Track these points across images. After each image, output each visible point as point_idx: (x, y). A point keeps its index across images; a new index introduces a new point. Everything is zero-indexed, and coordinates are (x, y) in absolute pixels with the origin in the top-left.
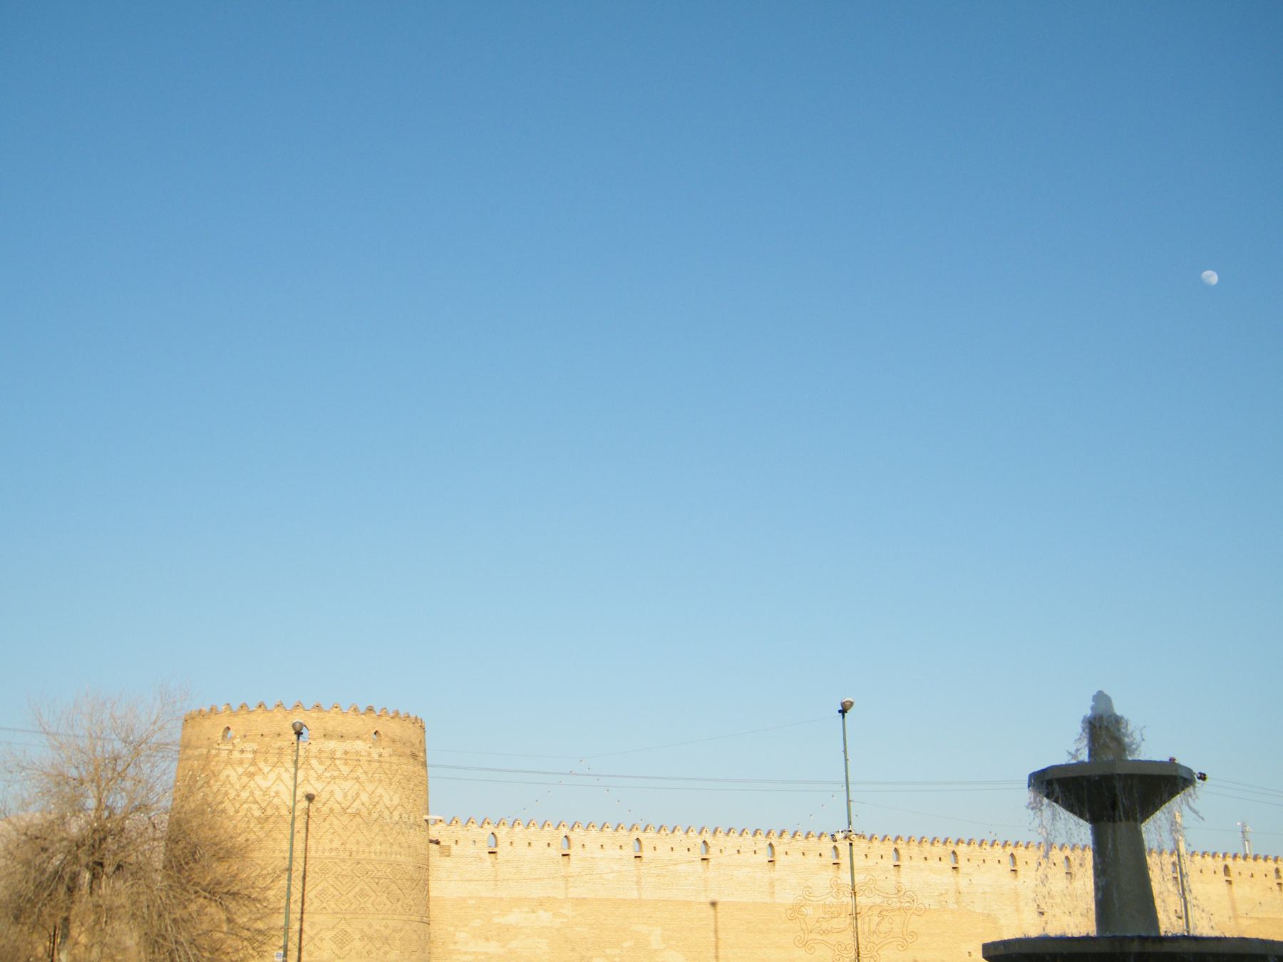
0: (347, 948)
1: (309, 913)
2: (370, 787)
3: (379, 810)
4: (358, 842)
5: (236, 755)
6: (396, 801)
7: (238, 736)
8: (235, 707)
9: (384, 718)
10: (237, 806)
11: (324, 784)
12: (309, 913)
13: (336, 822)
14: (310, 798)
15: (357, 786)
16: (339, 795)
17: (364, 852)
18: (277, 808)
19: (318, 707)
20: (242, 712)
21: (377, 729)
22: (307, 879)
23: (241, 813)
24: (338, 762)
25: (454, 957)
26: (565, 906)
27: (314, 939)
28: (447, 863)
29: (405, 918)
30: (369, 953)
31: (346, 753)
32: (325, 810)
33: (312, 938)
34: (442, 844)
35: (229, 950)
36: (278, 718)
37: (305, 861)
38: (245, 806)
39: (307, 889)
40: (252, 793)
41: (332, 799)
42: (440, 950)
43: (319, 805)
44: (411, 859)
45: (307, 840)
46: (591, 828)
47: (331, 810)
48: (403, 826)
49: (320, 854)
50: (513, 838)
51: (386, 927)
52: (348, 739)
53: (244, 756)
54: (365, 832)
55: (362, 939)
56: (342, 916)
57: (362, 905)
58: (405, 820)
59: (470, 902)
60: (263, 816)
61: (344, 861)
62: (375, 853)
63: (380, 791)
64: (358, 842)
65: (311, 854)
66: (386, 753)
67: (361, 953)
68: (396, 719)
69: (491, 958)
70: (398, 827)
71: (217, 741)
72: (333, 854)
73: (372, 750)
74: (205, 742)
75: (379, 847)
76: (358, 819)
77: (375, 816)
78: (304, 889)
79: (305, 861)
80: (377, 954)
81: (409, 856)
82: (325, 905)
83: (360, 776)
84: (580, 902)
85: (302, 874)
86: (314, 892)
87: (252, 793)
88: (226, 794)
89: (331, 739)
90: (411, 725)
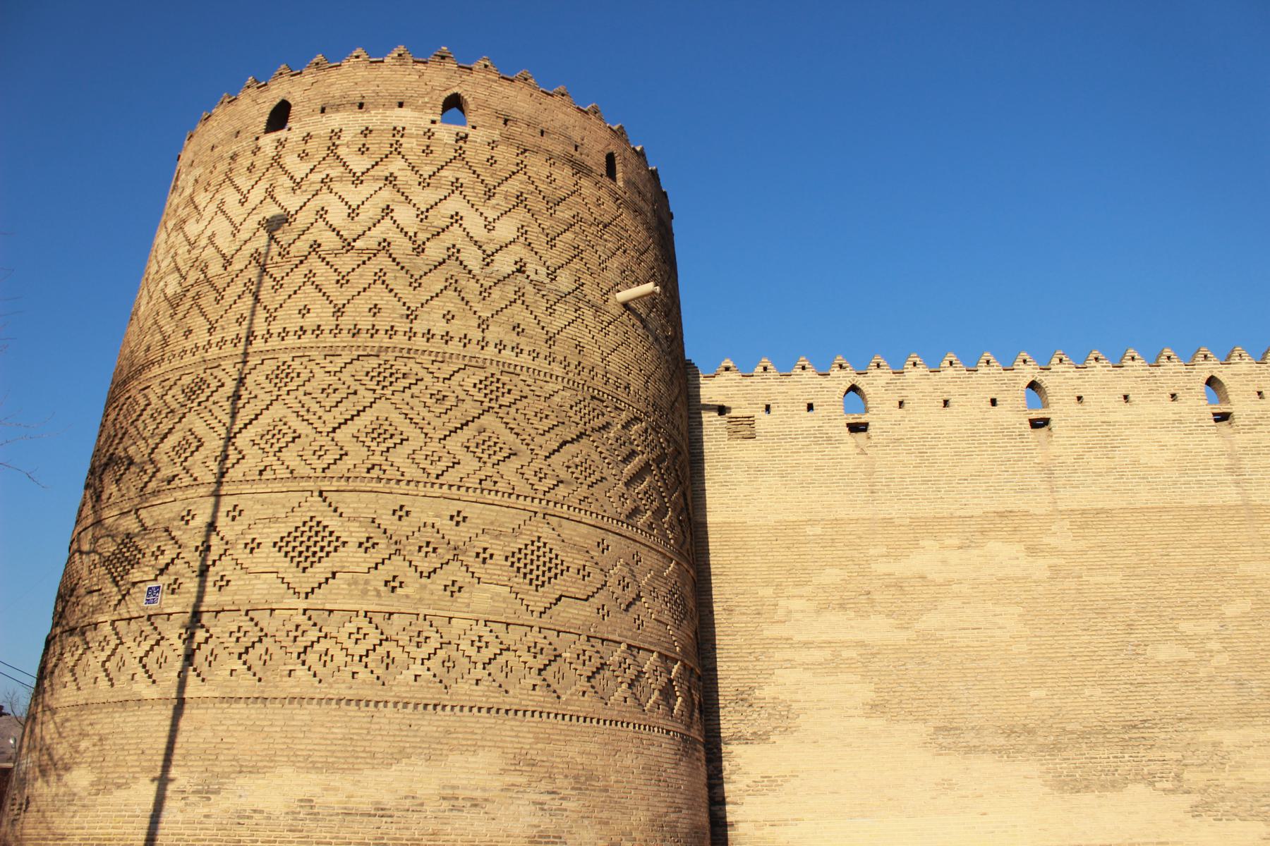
0: (320, 571)
2: (423, 198)
4: (375, 310)
6: (506, 229)
13: (320, 268)
16: (337, 215)
24: (342, 151)
25: (778, 656)
28: (746, 451)
30: (393, 584)
34: (733, 413)
42: (740, 641)
46: (1093, 363)
47: (315, 246)
50: (904, 393)
52: (376, 107)
55: (367, 545)
57: (377, 459)
59: (809, 530)
62: (429, 336)
67: (367, 582)
69: (874, 655)
76: (383, 260)
77: (435, 251)
84: (1087, 519)
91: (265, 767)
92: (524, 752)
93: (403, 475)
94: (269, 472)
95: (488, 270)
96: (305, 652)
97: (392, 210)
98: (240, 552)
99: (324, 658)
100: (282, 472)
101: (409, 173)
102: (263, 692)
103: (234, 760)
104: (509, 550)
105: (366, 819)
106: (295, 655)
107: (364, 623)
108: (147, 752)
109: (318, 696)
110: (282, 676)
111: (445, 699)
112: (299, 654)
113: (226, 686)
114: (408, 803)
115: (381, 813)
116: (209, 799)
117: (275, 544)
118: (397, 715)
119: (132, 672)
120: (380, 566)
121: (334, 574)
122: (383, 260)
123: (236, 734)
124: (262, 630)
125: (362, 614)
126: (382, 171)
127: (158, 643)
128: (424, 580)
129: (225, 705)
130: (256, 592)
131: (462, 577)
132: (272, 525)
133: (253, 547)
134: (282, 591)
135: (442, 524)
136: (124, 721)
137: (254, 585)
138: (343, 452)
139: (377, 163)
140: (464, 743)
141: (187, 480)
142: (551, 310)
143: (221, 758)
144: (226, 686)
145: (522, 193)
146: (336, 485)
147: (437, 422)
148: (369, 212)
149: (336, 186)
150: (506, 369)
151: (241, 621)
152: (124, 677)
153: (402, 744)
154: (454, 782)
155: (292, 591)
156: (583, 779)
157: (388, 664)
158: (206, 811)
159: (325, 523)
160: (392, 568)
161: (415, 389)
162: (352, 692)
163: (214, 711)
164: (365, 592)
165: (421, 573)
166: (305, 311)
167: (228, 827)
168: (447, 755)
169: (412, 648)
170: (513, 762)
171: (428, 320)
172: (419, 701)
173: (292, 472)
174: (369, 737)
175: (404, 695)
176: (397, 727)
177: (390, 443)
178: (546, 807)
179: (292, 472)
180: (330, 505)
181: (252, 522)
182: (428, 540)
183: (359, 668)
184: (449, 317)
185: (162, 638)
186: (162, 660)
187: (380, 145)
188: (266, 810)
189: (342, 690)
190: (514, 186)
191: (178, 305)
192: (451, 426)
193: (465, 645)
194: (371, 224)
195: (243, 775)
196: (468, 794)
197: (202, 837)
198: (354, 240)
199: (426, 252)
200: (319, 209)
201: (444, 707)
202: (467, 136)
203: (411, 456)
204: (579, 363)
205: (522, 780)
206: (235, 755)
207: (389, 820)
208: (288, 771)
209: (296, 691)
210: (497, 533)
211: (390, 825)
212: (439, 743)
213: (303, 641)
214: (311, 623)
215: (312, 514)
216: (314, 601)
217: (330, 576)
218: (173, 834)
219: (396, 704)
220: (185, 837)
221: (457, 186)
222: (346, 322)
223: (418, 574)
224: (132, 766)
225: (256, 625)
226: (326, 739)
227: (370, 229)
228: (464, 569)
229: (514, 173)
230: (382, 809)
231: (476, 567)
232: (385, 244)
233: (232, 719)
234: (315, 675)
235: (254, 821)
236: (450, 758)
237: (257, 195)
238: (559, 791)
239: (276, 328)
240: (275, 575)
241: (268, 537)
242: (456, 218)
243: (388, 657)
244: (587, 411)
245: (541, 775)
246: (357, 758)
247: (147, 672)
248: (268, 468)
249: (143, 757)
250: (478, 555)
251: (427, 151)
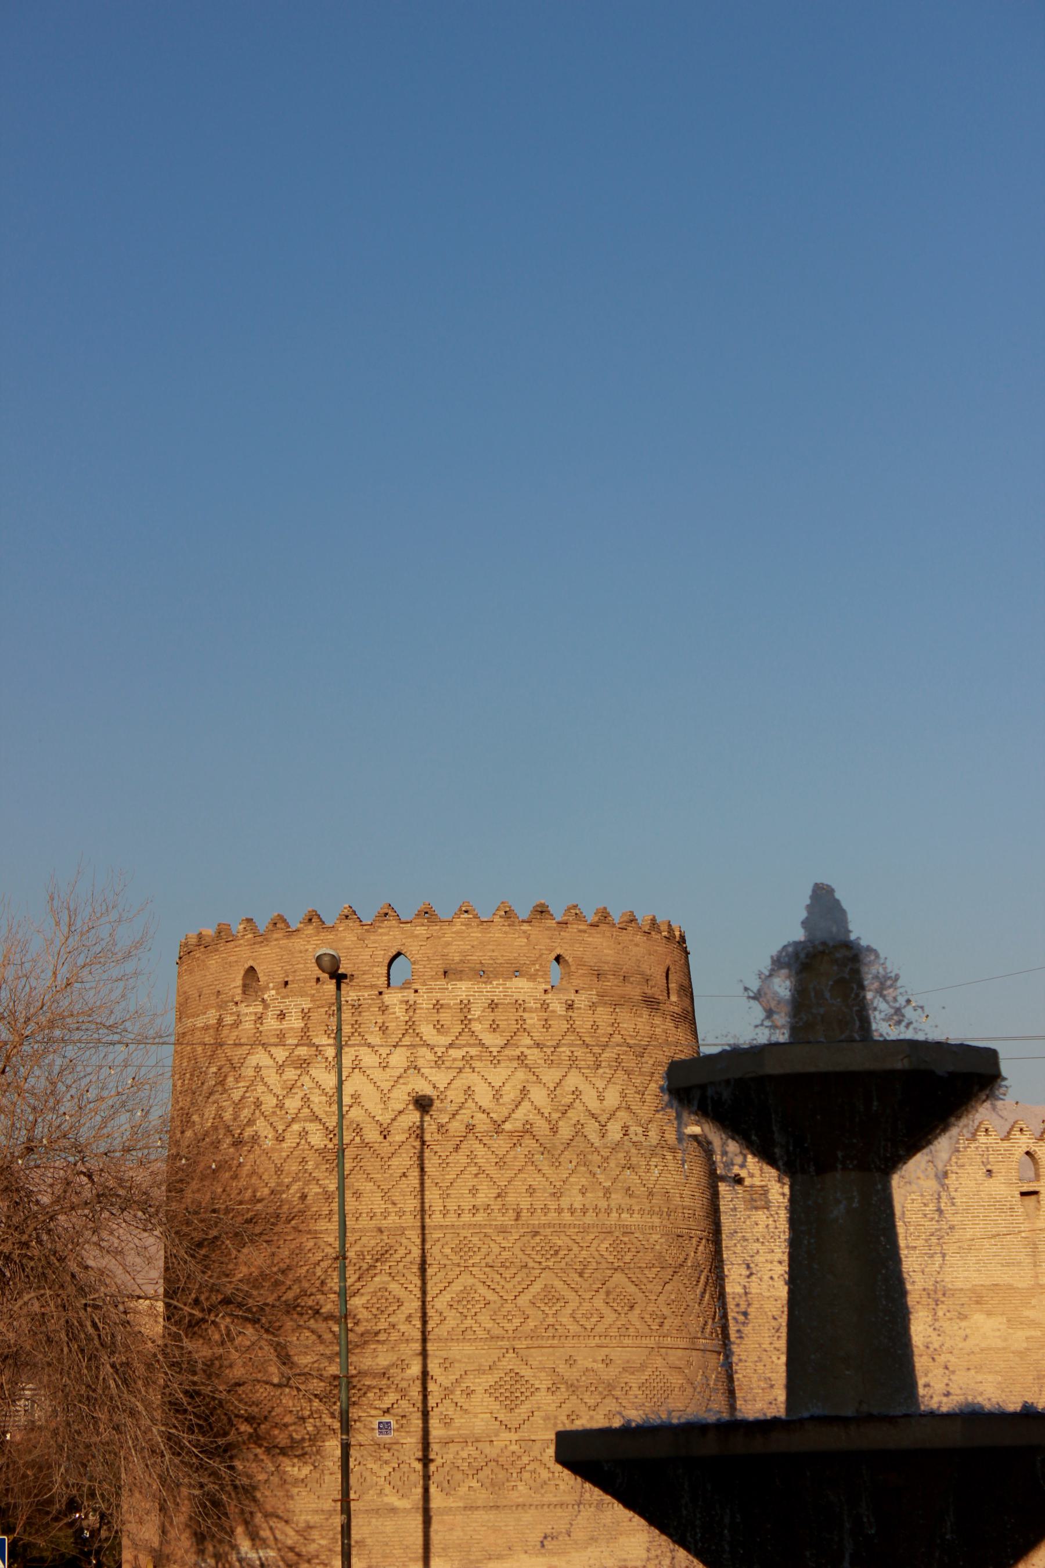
0: (524, 1410)
1: (439, 1339)
2: (550, 1076)
3: (573, 1122)
5: (271, 1023)
6: (612, 1098)
7: (271, 985)
8: (262, 925)
9: (573, 928)
10: (280, 1128)
11: (453, 1073)
12: (439, 1339)
13: (480, 1150)
14: (423, 1104)
15: (521, 1075)
16: (484, 1096)
17: (545, 1210)
18: (358, 1130)
19: (427, 914)
20: (275, 936)
21: (558, 951)
22: (430, 1271)
23: (289, 1143)
24: (476, 1027)
26: (1034, 1302)
27: (452, 1392)
29: (651, 1342)
31: (493, 1006)
32: (456, 1127)
33: (448, 1393)
35: (288, 1419)
36: (347, 943)
37: (423, 1234)
38: (296, 1127)
39: (432, 1291)
40: (306, 1099)
41: (470, 1104)
43: (444, 1119)
44: (656, 1220)
45: (422, 1190)
47: (470, 1128)
48: (633, 1151)
49: (451, 1219)
51: (607, 1362)
52: (496, 978)
53: (285, 1025)
54: (546, 1169)
55: (552, 1390)
56: (505, 1343)
57: (551, 1320)
58: (635, 1139)
60: (330, 1146)
61: (503, 1230)
62: (572, 1211)
63: (574, 1080)
64: (531, 1191)
65: (435, 1220)
66: (582, 1001)
67: (556, 1418)
68: (603, 927)
70: (621, 1155)
71: (233, 996)
72: (480, 1217)
73: (549, 996)
74: (213, 1000)
75: (580, 1198)
76: (528, 1141)
77: (565, 1131)
78: (424, 1292)
79: (423, 1234)
80: (592, 1418)
81: (651, 1213)
82: (469, 1322)
83: (527, 1052)
85: (418, 1260)
86: (446, 1297)
87: (306, 1099)
88: (258, 1104)
89: (461, 980)
90: (639, 938)
91: (507, 1555)
94: (469, 1332)
95: (605, 1140)
100: (481, 1334)
109: (536, 1503)
110: (508, 1490)
113: (468, 1499)
120: (563, 1405)
128: (592, 1413)
134: (497, 1427)
135: (598, 1368)
136: (382, 1525)
137: (474, 1422)
140: (628, 1528)
144: (468, 1499)
145: (619, 1055)
146: (524, 1344)
147: (585, 1285)
148: (510, 1094)
149: (476, 1064)
150: (625, 1230)
159: (531, 1382)
160: (570, 1405)
171: (570, 1196)
187: (507, 1019)
189: (550, 1498)
194: (513, 1107)
199: (560, 1132)
200: (466, 1088)
206: (483, 1547)
208: (523, 1556)
215: (511, 1367)
216: (522, 1434)
236: (621, 1540)
237: (399, 1059)
241: (480, 1385)
246: (566, 1545)
248: (469, 1330)
249: (408, 1550)
251: (547, 1026)
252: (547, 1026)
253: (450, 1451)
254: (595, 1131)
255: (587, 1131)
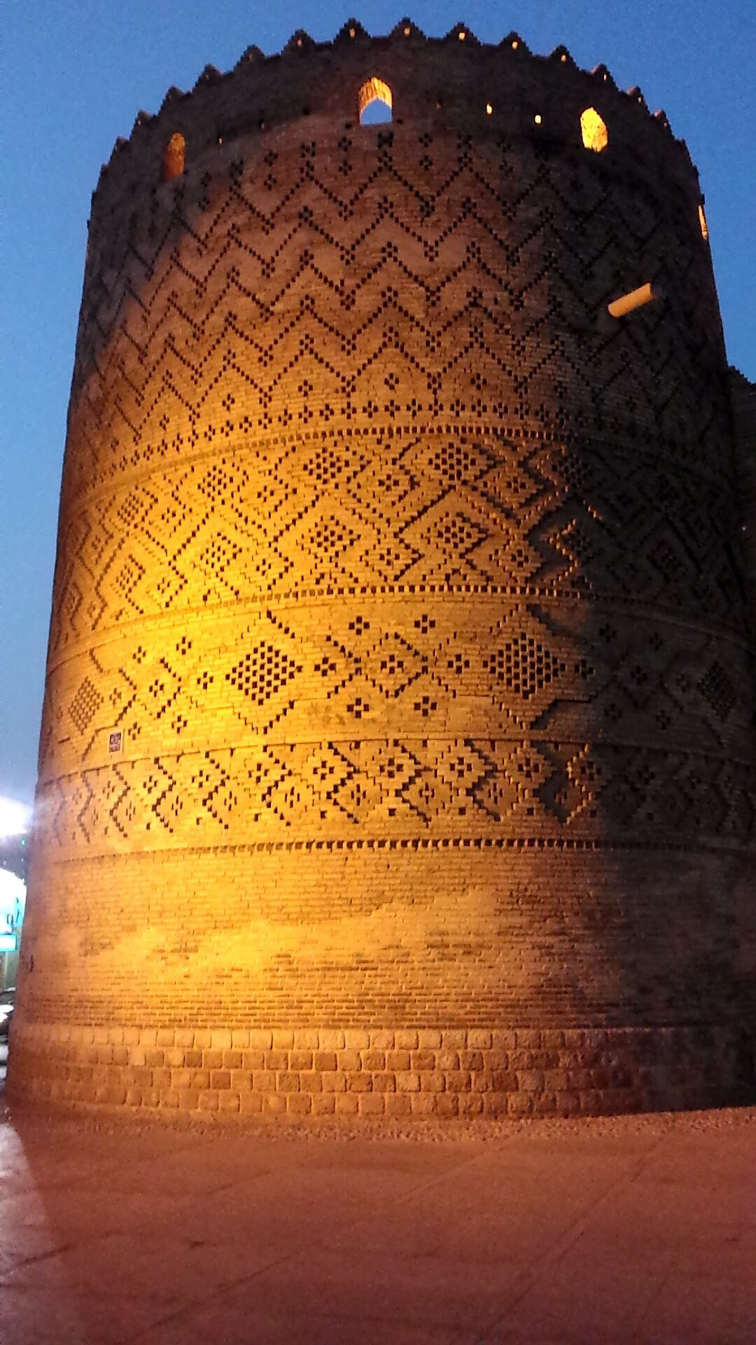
0: (276, 702)
2: (345, 232)
15: (302, 236)
17: (327, 412)
47: (231, 318)
55: (325, 667)
57: (326, 567)
62: (371, 410)
77: (366, 301)
81: (523, 411)
83: (311, 206)
92: (522, 887)
93: (356, 581)
96: (269, 792)
97: (312, 257)
98: (193, 689)
99: (289, 798)
100: (228, 596)
101: (326, 202)
102: (230, 840)
103: (208, 915)
104: (489, 652)
105: (347, 973)
106: (260, 797)
107: (328, 755)
108: (127, 910)
111: (425, 833)
112: (264, 797)
114: (392, 953)
115: (364, 966)
116: (188, 958)
117: (228, 677)
118: (373, 856)
119: (105, 826)
121: (292, 704)
122: (309, 323)
123: (207, 887)
124: (223, 772)
125: (325, 745)
126: (294, 207)
127: (125, 794)
128: (390, 700)
129: (195, 857)
130: (214, 731)
131: (433, 692)
132: (222, 655)
133: (205, 682)
137: (212, 723)
138: (288, 564)
139: (287, 198)
141: (134, 613)
142: (519, 350)
143: (195, 913)
149: (245, 238)
151: (202, 764)
152: (99, 832)
153: (381, 888)
154: (442, 927)
155: (249, 727)
156: (598, 916)
157: (358, 799)
158: (185, 970)
161: (361, 478)
162: (322, 833)
163: (184, 863)
164: (327, 721)
165: (387, 692)
166: (228, 402)
167: (208, 987)
168: (433, 898)
169: (383, 779)
170: (510, 900)
172: (395, 838)
173: (237, 593)
174: (345, 882)
175: (379, 832)
176: (374, 868)
177: (339, 546)
178: (553, 951)
179: (237, 593)
180: (280, 626)
181: (202, 654)
182: (391, 653)
183: (328, 806)
184: (392, 382)
185: (129, 788)
186: (131, 811)
188: (245, 968)
190: (459, 190)
191: (101, 412)
192: (406, 515)
193: (443, 770)
195: (217, 931)
196: (459, 939)
197: (184, 998)
198: (273, 304)
201: (425, 844)
202: (391, 136)
203: (363, 559)
204: (561, 410)
205: (524, 920)
207: (373, 973)
208: (262, 924)
209: (263, 838)
210: (472, 635)
211: (373, 980)
212: (422, 883)
213: (267, 782)
214: (273, 760)
217: (287, 705)
218: (157, 996)
219: (371, 844)
220: (168, 999)
221: (385, 207)
222: (276, 408)
223: (384, 694)
224: (114, 925)
225: (218, 767)
226: (299, 887)
227: (288, 286)
228: (436, 681)
229: (456, 174)
230: (364, 962)
231: (449, 678)
232: (309, 302)
233: (202, 871)
234: (282, 818)
235: (233, 980)
238: (569, 931)
239: (201, 428)
240: (230, 711)
241: (219, 669)
242: (390, 250)
243: (358, 790)
244: (574, 470)
245: (546, 914)
247: (118, 825)
250: (450, 664)
251: (346, 168)
252: (346, 168)
253: (181, 768)
254: (418, 299)
255: (403, 299)
